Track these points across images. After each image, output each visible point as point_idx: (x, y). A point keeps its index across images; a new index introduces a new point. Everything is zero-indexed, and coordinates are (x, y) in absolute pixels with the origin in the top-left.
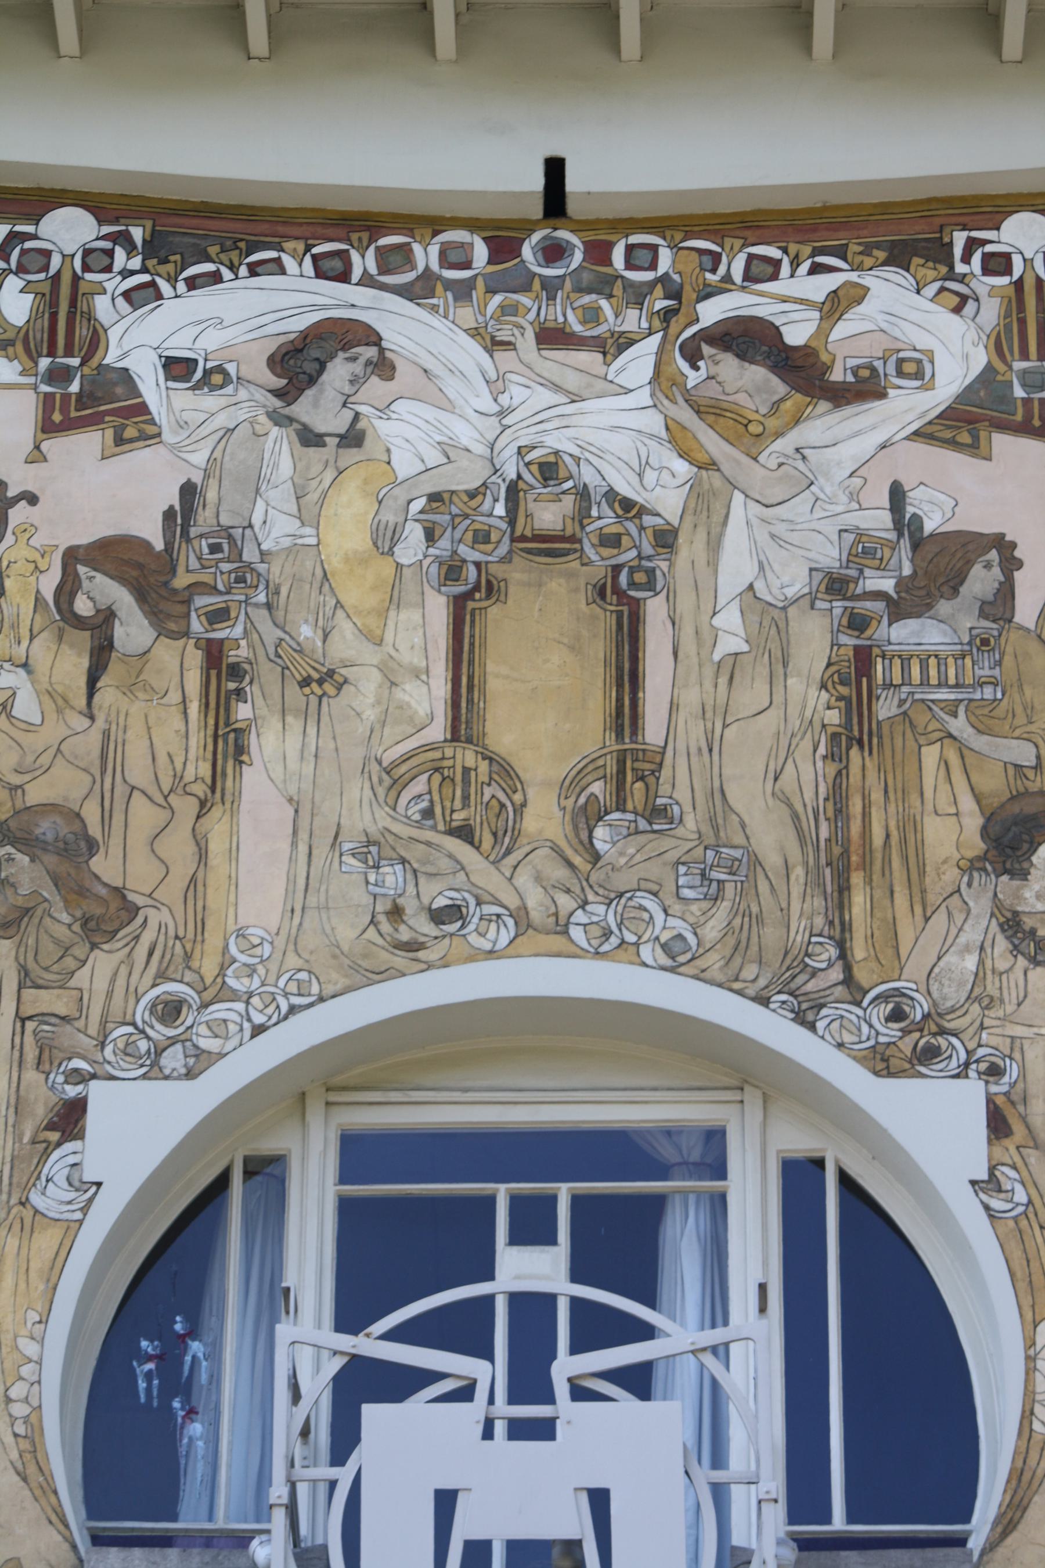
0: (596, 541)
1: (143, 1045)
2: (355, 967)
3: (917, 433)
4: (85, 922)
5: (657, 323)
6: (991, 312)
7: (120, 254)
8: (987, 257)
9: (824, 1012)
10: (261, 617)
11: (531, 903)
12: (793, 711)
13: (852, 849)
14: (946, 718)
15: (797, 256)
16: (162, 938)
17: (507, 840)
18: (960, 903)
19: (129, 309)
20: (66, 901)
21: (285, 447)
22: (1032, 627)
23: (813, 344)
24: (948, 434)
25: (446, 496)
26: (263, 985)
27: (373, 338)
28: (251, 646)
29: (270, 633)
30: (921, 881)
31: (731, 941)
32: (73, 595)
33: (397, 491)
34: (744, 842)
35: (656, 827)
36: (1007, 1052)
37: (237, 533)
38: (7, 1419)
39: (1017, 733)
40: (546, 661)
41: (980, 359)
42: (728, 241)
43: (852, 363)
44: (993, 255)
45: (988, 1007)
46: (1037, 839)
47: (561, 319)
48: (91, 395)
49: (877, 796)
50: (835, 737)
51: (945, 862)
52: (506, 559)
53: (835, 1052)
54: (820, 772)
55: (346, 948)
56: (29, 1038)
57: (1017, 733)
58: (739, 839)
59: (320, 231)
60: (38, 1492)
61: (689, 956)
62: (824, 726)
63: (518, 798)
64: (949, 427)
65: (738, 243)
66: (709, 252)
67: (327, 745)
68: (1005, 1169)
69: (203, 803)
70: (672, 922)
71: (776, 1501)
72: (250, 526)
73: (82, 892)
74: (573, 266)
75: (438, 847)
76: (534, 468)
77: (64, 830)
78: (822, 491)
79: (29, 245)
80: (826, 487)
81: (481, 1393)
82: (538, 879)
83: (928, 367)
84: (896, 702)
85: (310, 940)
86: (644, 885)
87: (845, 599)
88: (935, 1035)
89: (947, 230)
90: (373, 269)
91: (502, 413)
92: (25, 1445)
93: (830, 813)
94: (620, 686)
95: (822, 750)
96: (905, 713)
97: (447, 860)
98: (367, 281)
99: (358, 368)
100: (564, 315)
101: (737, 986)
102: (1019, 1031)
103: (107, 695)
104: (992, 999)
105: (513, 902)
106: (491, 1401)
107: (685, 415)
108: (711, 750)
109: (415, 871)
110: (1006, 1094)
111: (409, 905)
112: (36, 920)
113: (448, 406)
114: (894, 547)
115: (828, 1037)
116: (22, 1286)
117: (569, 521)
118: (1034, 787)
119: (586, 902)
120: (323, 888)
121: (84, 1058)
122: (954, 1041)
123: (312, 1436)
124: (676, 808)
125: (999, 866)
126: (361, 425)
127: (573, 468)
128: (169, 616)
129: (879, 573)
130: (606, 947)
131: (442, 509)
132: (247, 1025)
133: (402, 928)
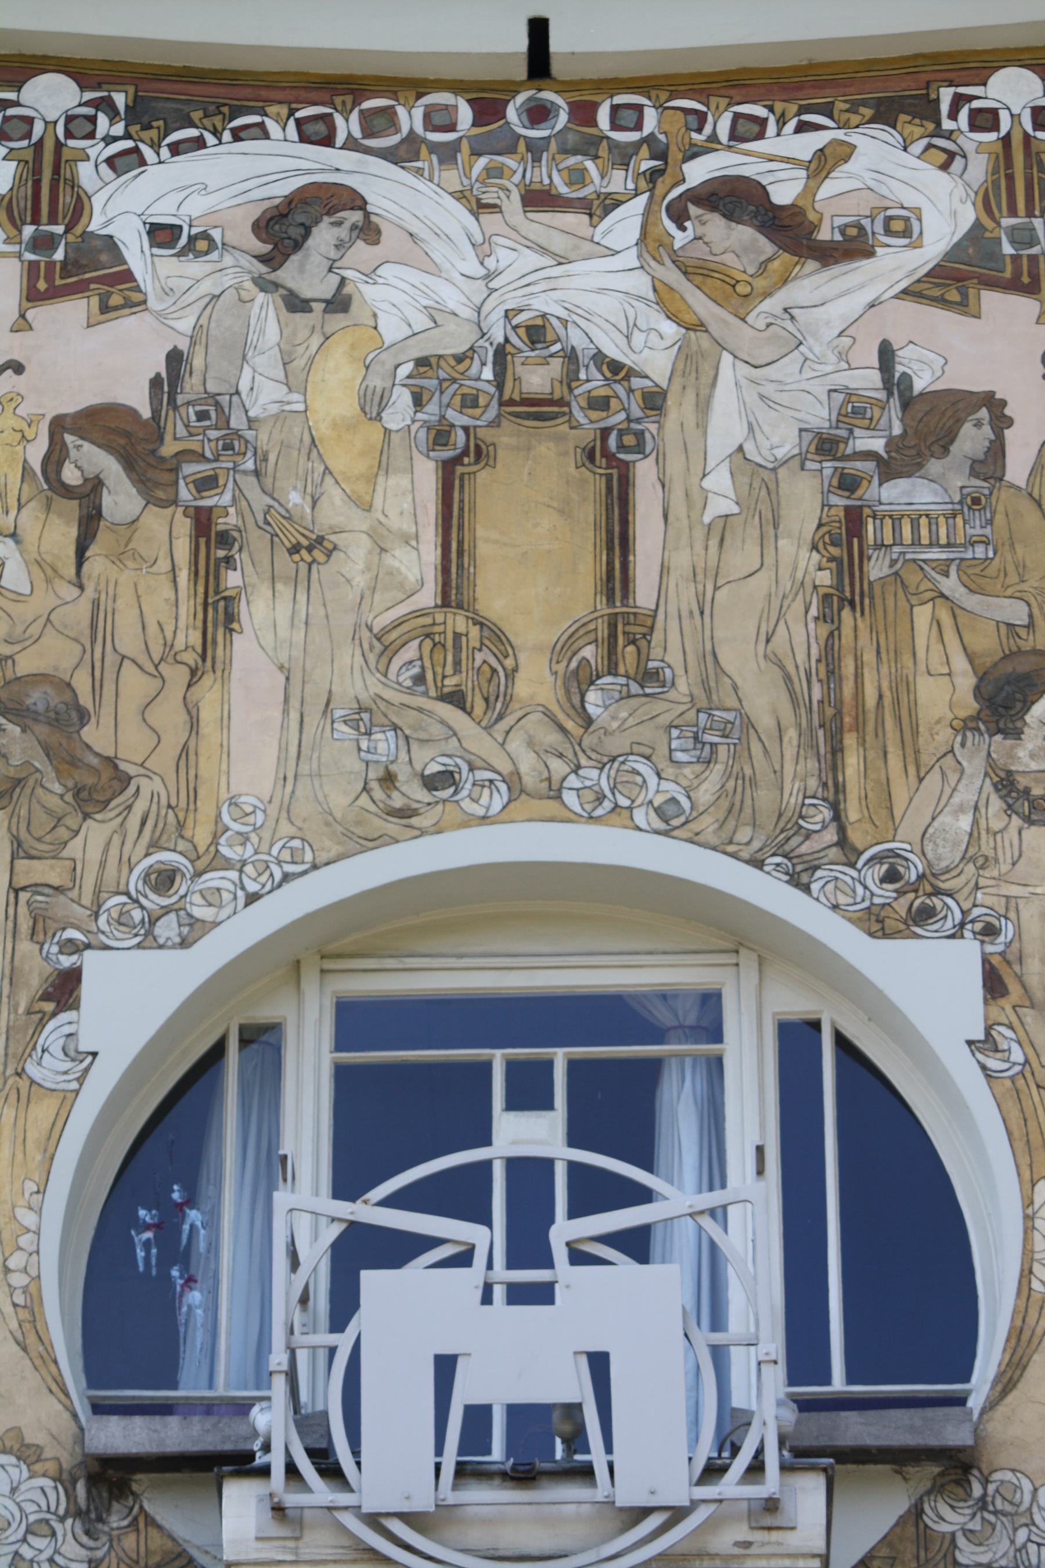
0: (584, 404)
1: (137, 915)
2: (348, 834)
3: (905, 292)
4: (77, 795)
5: (643, 184)
6: (978, 169)
7: (102, 120)
8: (974, 113)
9: (819, 873)
10: (249, 484)
11: (524, 768)
12: (784, 573)
13: (845, 710)
14: (938, 577)
15: (783, 115)
16: (154, 807)
17: (499, 705)
18: (953, 763)
19: (112, 175)
20: (57, 771)
21: (272, 313)
22: (1023, 485)
23: (800, 204)
24: (936, 293)
25: (433, 361)
26: (256, 853)
27: (358, 202)
28: (240, 513)
29: (259, 501)
30: (915, 742)
31: (725, 804)
32: (60, 465)
33: (384, 356)
34: (736, 705)
35: (648, 691)
36: (1002, 912)
37: (224, 400)
38: (6, 1289)
39: (1009, 592)
40: (536, 525)
41: (968, 216)
42: (714, 101)
43: (839, 221)
44: (980, 111)
45: (982, 867)
46: (1030, 698)
47: (546, 181)
48: (76, 263)
49: (869, 657)
50: (826, 598)
51: (938, 722)
52: (495, 423)
53: (830, 913)
54: (812, 634)
55: (338, 815)
56: (23, 909)
57: (1009, 592)
58: (731, 702)
59: (303, 94)
60: (38, 1362)
61: (682, 819)
62: (815, 587)
63: (509, 663)
64: (937, 285)
65: (723, 102)
66: (695, 112)
68: (1001, 1029)
69: (193, 672)
70: (665, 785)
71: (775, 1362)
72: (238, 393)
73: (74, 762)
74: (559, 126)
75: (430, 713)
76: (522, 332)
77: (55, 700)
78: (810, 350)
79: (11, 112)
80: (814, 347)
81: (480, 1258)
82: (531, 744)
83: (915, 224)
84: (887, 562)
85: (303, 808)
86: (636, 749)
87: (835, 459)
88: (929, 895)
89: (934, 86)
90: (357, 133)
91: (489, 276)
92: (24, 1314)
93: (823, 675)
94: (610, 549)
95: (814, 612)
96: (896, 574)
97: (439, 726)
98: (351, 144)
99: (343, 232)
100: (550, 177)
101: (731, 849)
102: (1014, 890)
103: (96, 564)
104: (986, 858)
105: (506, 767)
106: (490, 1266)
107: (672, 276)
108: (702, 613)
109: (407, 738)
110: (1002, 954)
111: (402, 771)
112: (28, 791)
113: (435, 270)
114: (883, 407)
115: (822, 899)
116: (19, 1156)
117: (557, 385)
118: (1026, 646)
119: (579, 767)
120: (315, 756)
121: (78, 928)
122: (949, 901)
123: (311, 1303)
124: (668, 671)
125: (993, 726)
126: (348, 289)
127: (561, 331)
128: (157, 484)
129: (869, 433)
130: (599, 812)
131: (430, 373)
132: (240, 894)
133: (395, 794)
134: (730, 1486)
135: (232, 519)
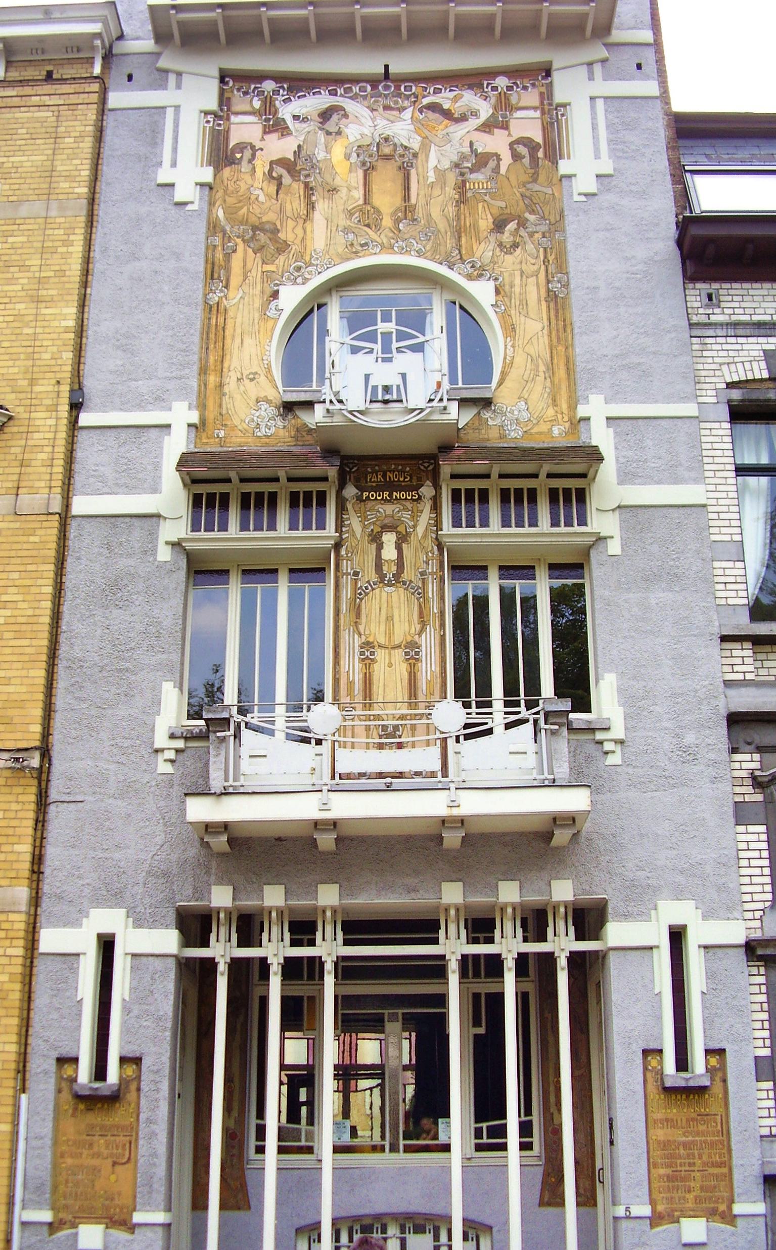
6: (493, 100)
7: (281, 91)
10: (318, 176)
27: (344, 110)
29: (320, 180)
41: (491, 111)
49: (467, 215)
67: (334, 205)
73: (277, 242)
85: (332, 252)
98: (341, 96)
103: (281, 196)
107: (420, 126)
111: (355, 243)
113: (362, 125)
134: (434, 404)
135: (314, 184)
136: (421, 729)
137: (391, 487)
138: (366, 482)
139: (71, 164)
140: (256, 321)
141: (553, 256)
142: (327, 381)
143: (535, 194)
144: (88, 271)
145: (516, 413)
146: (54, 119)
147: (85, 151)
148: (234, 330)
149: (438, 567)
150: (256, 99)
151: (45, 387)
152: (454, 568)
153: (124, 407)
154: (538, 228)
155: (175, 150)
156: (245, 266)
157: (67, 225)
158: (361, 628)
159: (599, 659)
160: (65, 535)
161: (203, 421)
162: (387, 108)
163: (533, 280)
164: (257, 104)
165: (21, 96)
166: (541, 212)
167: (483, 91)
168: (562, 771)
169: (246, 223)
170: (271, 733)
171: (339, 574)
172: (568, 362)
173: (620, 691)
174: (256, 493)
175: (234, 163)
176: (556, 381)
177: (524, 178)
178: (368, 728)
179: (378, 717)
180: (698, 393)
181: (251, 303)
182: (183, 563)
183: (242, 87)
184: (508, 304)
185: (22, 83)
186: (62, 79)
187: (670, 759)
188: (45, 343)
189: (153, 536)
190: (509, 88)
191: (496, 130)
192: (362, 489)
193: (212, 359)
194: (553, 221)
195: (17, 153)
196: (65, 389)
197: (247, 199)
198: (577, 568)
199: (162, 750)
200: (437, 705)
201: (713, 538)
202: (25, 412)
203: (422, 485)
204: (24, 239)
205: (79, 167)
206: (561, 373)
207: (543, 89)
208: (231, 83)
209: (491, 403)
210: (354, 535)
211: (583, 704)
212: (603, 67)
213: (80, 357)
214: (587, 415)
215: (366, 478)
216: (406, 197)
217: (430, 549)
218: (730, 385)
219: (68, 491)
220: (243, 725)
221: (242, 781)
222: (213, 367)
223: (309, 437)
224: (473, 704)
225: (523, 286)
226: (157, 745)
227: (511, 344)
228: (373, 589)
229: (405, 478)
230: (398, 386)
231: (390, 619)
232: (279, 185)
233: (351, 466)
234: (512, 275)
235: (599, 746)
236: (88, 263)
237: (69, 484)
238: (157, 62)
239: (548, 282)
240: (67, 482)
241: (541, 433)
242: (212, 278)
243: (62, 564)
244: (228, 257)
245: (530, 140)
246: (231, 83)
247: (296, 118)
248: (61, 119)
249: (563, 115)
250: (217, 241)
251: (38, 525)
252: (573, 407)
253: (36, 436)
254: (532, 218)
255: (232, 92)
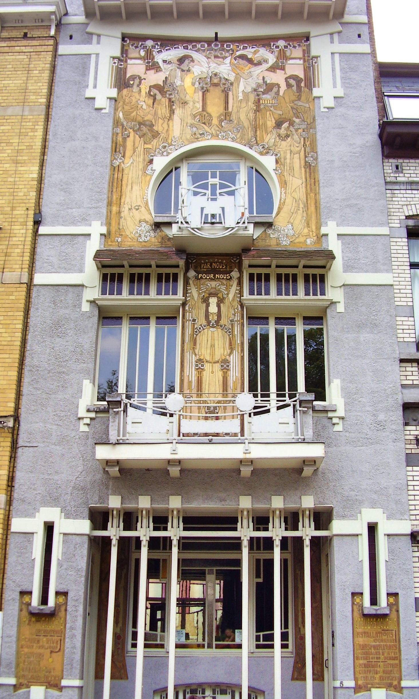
1: (161, 152)
4: (153, 136)
6: (276, 54)
7: (157, 46)
8: (276, 46)
10: (176, 95)
11: (213, 133)
12: (249, 107)
27: (192, 57)
29: (178, 97)
41: (275, 60)
49: (261, 118)
50: (255, 110)
52: (210, 87)
58: (242, 124)
73: (152, 131)
81: (207, 195)
82: (214, 129)
85: (183, 138)
90: (191, 48)
91: (209, 67)
98: (190, 49)
102: (280, 150)
103: (155, 105)
105: (211, 133)
111: (197, 133)
113: (201, 66)
114: (263, 85)
118: (282, 117)
134: (240, 225)
135: (174, 99)
136: (229, 409)
137: (215, 271)
138: (201, 268)
139: (37, 86)
140: (140, 176)
141: (309, 143)
142: (180, 211)
143: (299, 107)
144: (45, 146)
145: (286, 231)
146: (28, 60)
147: (45, 78)
148: (128, 181)
149: (241, 318)
150: (142, 50)
151: (20, 211)
152: (249, 318)
153: (64, 224)
154: (300, 126)
155: (96, 78)
156: (134, 145)
157: (34, 120)
158: (197, 351)
159: (331, 371)
160: (30, 296)
161: (109, 232)
162: (216, 57)
163: (297, 156)
164: (143, 53)
165: (9, 47)
166: (302, 117)
167: (271, 48)
168: (309, 434)
169: (136, 121)
170: (145, 410)
171: (185, 320)
172: (316, 202)
173: (342, 389)
174: (138, 274)
175: (129, 87)
176: (309, 213)
177: (293, 98)
178: (199, 408)
179: (205, 402)
180: (390, 221)
181: (137, 166)
182: (96, 313)
183: (134, 44)
184: (283, 169)
185: (10, 39)
186: (33, 37)
187: (370, 428)
188: (20, 187)
189: (79, 297)
190: (286, 47)
191: (278, 71)
192: (198, 272)
193: (114, 197)
194: (309, 122)
195: (6, 79)
196: (31, 213)
197: (136, 107)
198: (319, 319)
199: (82, 418)
200: (238, 395)
201: (397, 303)
202: (8, 225)
203: (232, 271)
204: (10, 127)
205: (41, 87)
206: (312, 209)
207: (305, 48)
208: (128, 41)
209: (272, 225)
210: (193, 299)
211: (321, 396)
212: (339, 36)
213: (40, 195)
214: (326, 233)
215: (201, 266)
216: (226, 108)
217: (236, 307)
218: (408, 217)
219: (32, 270)
220: (128, 405)
221: (127, 436)
222: (115, 202)
223: (169, 243)
224: (259, 395)
225: (292, 159)
226: (80, 415)
227: (284, 192)
228: (204, 329)
229: (223, 266)
230: (220, 215)
231: (213, 346)
232: (155, 100)
233: (192, 259)
234: (285, 153)
235: (330, 420)
236: (45, 142)
237: (33, 267)
238: (86, 28)
239: (306, 157)
240: (31, 266)
241: (300, 243)
242: (116, 151)
243: (28, 312)
244: (125, 140)
245: (297, 76)
246: (128, 41)
247: (164, 61)
248: (31, 60)
249: (315, 63)
250: (119, 130)
251: (14, 290)
252: (318, 228)
253: (14, 239)
254: (297, 120)
255: (129, 46)
